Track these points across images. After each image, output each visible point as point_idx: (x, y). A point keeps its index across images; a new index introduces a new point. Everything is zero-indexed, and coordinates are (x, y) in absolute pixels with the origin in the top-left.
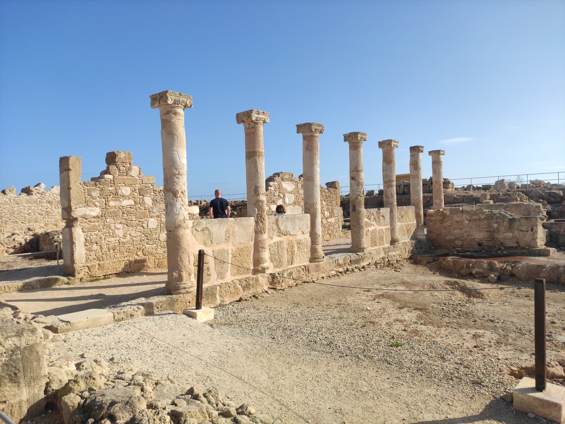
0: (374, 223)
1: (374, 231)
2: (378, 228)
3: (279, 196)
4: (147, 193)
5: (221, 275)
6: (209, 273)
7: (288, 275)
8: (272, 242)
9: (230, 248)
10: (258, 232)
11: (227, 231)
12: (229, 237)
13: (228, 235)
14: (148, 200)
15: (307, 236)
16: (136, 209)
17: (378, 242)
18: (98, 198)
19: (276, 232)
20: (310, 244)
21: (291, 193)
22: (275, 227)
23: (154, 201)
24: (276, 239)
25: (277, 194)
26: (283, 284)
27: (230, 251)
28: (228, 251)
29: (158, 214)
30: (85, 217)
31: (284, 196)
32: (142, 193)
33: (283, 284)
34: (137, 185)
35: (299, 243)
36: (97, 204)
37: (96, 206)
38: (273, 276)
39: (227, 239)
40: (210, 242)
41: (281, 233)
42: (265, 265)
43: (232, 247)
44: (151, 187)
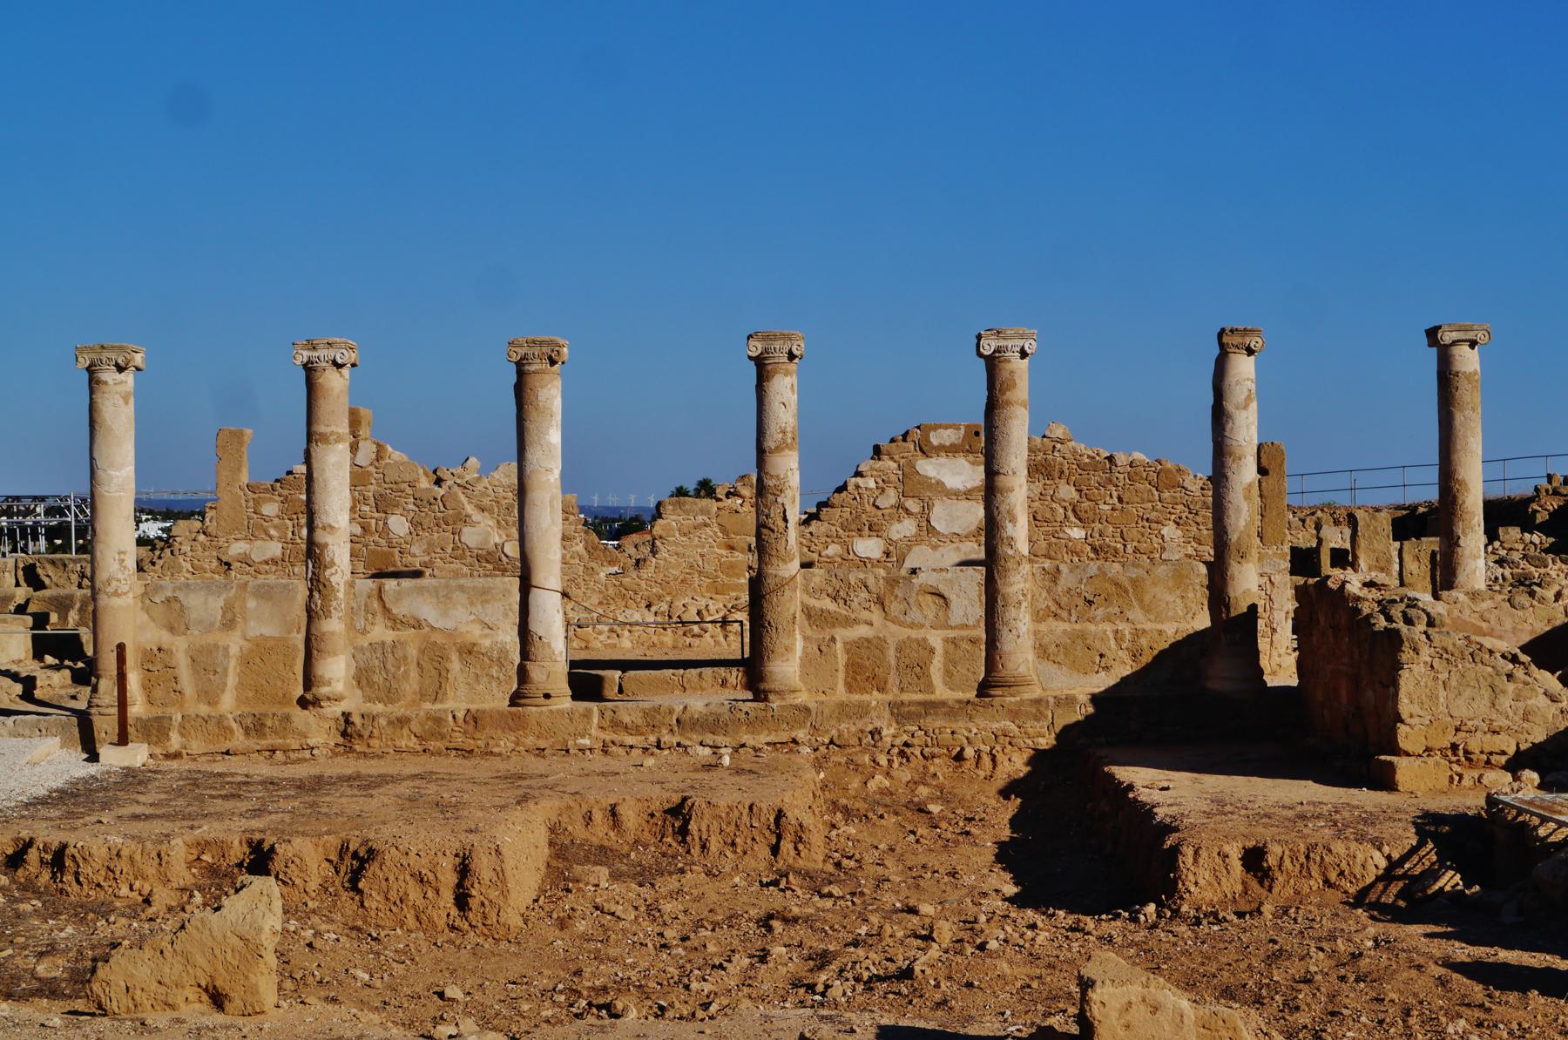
0: (876, 615)
1: (874, 645)
2: (896, 634)
3: (900, 506)
4: (397, 506)
5: (209, 696)
6: (178, 688)
7: (390, 723)
8: (364, 642)
9: (235, 644)
10: (311, 615)
11: (228, 608)
12: (232, 621)
13: (229, 616)
14: (398, 525)
15: (509, 637)
16: (366, 546)
17: (893, 680)
18: (276, 521)
19: (379, 619)
20: (517, 660)
21: (968, 495)
22: (376, 605)
23: (416, 524)
24: (380, 632)
25: (890, 499)
26: (375, 743)
27: (234, 650)
28: (226, 649)
29: (427, 559)
30: (245, 560)
31: (927, 508)
32: (382, 505)
33: (375, 743)
34: (371, 488)
35: (469, 651)
36: (273, 532)
37: (271, 538)
38: (346, 716)
39: (229, 624)
40: (183, 628)
41: (395, 622)
42: (324, 691)
43: (242, 642)
44: (409, 490)
